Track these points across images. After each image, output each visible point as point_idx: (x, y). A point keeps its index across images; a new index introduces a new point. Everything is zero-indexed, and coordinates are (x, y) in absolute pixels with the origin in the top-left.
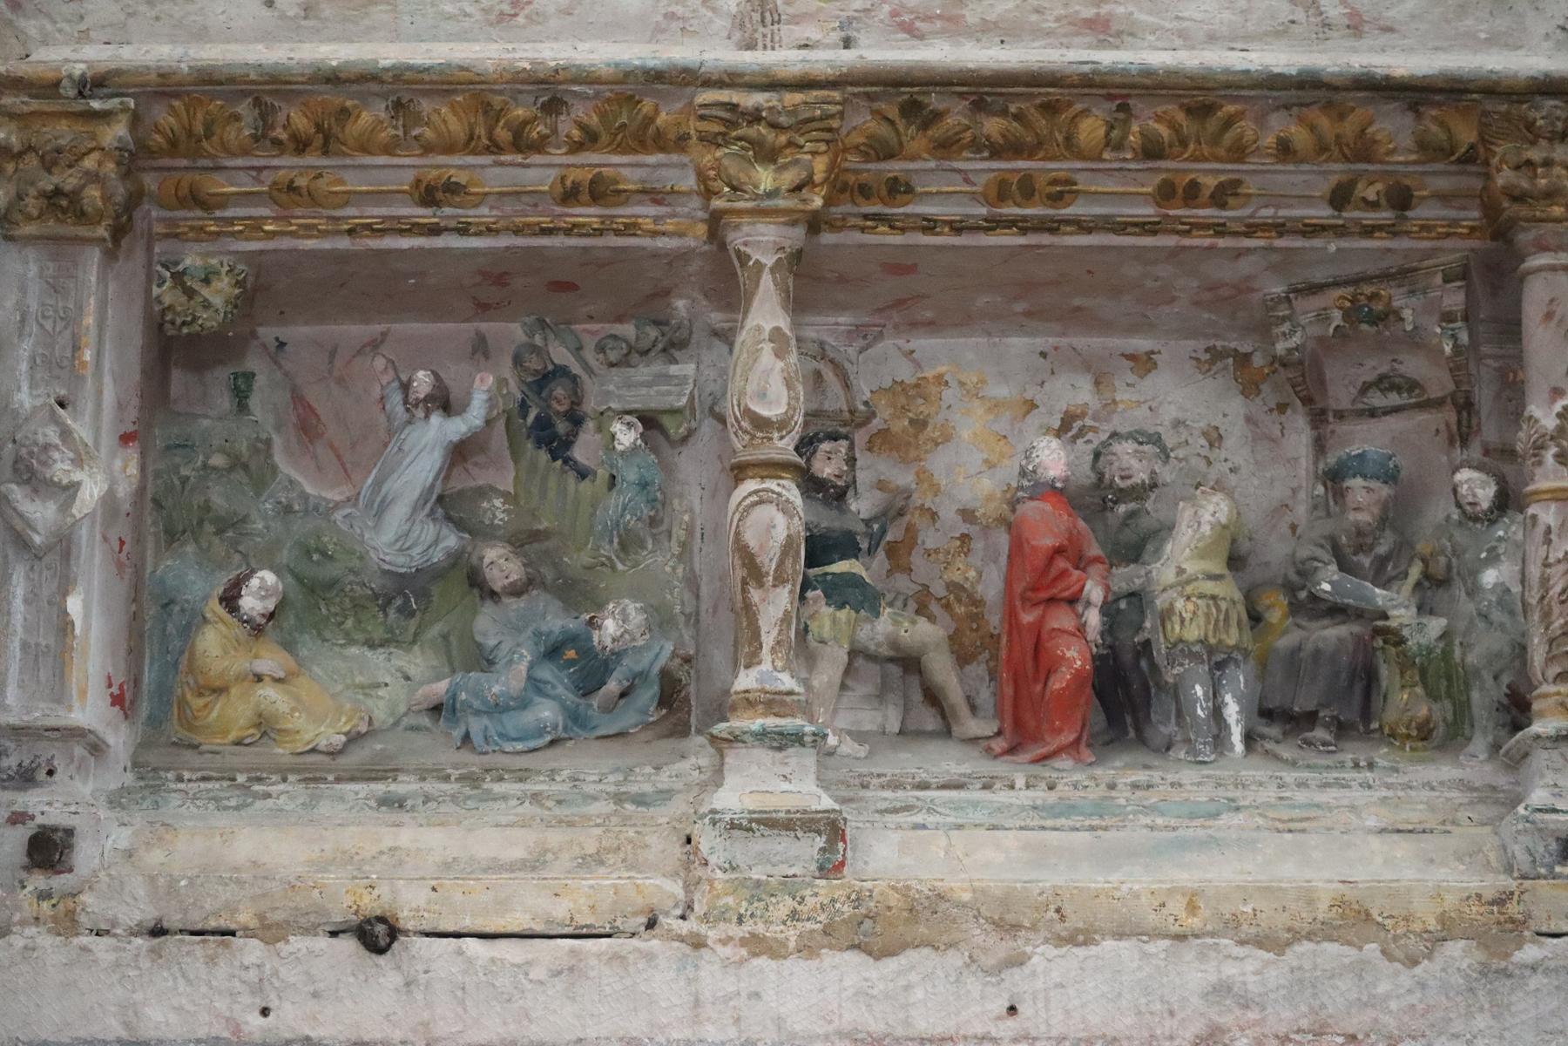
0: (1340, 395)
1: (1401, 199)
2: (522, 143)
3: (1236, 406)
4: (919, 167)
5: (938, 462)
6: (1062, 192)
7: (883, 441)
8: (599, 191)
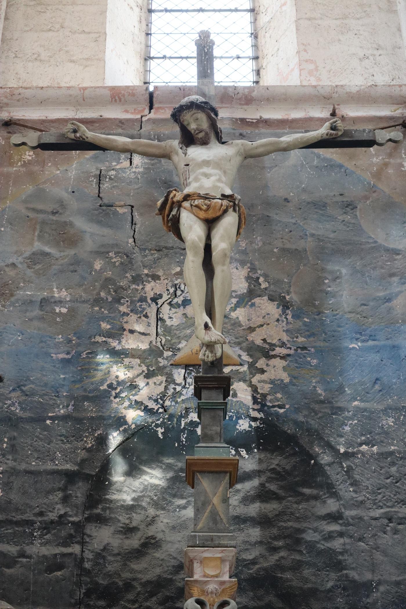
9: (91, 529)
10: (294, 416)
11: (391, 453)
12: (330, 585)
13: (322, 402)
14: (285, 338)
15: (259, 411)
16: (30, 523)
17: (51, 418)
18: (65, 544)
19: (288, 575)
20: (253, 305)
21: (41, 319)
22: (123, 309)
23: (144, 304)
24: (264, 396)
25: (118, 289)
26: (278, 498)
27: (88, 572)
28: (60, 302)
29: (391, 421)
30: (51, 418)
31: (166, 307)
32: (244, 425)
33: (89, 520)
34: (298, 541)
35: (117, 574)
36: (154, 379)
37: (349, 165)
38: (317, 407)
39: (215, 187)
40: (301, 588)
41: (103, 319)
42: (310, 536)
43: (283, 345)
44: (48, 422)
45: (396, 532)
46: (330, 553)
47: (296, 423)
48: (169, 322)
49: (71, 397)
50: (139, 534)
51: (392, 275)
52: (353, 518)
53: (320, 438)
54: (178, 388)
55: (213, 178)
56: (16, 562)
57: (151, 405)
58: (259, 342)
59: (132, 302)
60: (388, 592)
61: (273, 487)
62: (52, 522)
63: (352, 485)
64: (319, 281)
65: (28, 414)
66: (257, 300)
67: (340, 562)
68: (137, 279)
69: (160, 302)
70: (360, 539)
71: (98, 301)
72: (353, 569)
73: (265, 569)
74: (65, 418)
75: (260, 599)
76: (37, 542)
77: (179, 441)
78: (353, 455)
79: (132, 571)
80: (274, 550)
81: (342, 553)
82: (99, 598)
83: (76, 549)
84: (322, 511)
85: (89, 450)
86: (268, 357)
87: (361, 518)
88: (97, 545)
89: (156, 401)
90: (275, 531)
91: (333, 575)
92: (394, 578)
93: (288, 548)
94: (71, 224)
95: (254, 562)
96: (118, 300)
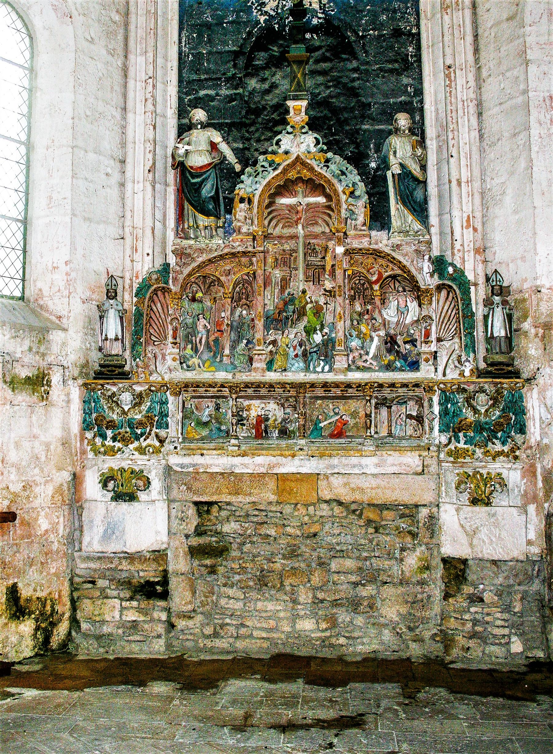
0: (286, 406)
1: (289, 391)
2: (214, 387)
5: (251, 412)
8: (221, 391)
10: (338, 16)
11: (384, 35)
12: (352, 104)
13: (352, 7)
15: (322, 13)
16: (220, 79)
17: (226, 23)
18: (236, 89)
19: (334, 100)
24: (325, 5)
26: (330, 60)
27: (246, 102)
30: (226, 23)
32: (315, 21)
33: (245, 76)
34: (339, 83)
35: (259, 102)
42: (344, 80)
44: (225, 25)
45: (383, 77)
46: (353, 88)
47: (340, 20)
49: (233, 11)
52: (364, 70)
56: (215, 99)
57: (272, 13)
60: (379, 108)
61: (328, 54)
62: (230, 77)
63: (364, 53)
65: (215, 22)
70: (368, 81)
72: (364, 97)
73: (324, 97)
75: (322, 112)
77: (285, 31)
78: (366, 36)
79: (265, 100)
80: (328, 87)
81: (358, 89)
83: (240, 91)
84: (350, 66)
85: (244, 39)
88: (250, 88)
89: (274, 10)
93: (335, 86)
95: (319, 94)
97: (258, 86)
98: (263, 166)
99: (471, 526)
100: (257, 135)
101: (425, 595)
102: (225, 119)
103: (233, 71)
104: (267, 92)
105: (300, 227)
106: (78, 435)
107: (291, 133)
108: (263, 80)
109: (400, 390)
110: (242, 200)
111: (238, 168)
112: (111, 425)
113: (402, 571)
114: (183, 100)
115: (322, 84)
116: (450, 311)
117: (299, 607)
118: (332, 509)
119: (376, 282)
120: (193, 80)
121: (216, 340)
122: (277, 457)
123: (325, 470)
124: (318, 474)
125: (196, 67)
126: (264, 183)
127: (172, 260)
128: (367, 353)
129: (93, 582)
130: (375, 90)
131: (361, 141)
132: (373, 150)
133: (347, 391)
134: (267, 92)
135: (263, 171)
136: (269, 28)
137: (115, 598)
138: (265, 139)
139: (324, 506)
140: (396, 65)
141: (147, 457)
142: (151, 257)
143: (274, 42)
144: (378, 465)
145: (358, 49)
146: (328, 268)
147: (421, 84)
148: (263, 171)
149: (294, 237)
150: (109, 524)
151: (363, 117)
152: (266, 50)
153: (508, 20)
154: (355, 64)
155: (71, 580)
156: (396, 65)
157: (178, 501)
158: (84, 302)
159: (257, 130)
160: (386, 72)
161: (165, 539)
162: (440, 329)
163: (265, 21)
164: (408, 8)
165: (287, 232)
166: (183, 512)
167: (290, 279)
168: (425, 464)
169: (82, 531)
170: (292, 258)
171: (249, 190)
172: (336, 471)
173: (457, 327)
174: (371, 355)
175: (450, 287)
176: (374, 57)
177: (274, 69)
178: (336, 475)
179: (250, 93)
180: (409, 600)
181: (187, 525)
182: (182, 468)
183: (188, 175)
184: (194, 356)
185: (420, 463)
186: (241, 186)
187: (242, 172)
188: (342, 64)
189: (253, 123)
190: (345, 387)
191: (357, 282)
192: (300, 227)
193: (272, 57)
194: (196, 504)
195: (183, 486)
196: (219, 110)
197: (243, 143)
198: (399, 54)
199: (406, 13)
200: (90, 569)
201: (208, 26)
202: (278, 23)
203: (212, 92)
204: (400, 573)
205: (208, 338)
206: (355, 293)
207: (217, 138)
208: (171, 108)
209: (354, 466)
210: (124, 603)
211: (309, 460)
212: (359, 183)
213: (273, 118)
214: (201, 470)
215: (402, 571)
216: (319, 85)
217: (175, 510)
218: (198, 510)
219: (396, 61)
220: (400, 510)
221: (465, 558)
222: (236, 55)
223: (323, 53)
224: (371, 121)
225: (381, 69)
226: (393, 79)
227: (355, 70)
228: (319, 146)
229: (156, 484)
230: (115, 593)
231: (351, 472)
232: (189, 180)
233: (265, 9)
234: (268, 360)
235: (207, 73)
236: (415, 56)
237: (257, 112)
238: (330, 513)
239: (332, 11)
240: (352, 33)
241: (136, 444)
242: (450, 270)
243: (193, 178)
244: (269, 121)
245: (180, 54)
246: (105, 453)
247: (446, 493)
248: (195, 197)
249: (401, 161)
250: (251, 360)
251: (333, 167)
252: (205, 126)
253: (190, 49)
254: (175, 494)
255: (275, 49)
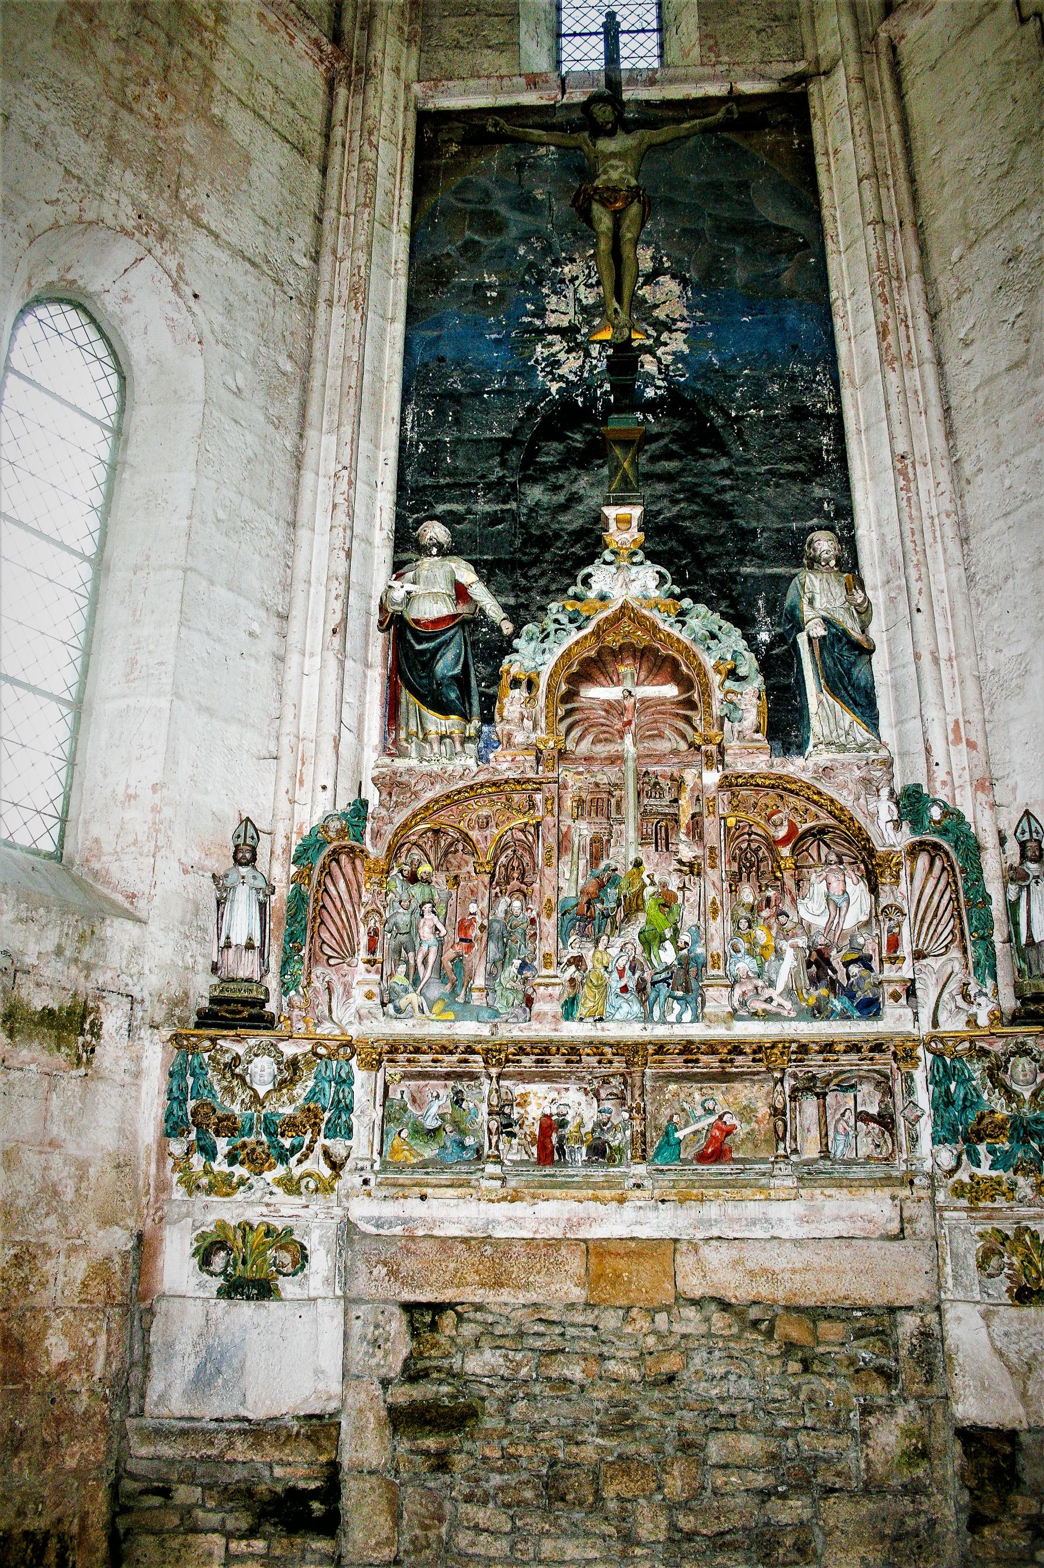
1: (610, 1062)
2: (451, 1053)
3: (584, 1098)
4: (523, 1058)
5: (528, 1109)
6: (547, 1062)
7: (518, 1105)
8: (466, 1061)
9: (526, 488)
10: (692, 384)
11: (776, 417)
12: (722, 531)
13: (717, 371)
14: (685, 313)
17: (488, 393)
18: (505, 502)
20: (657, 283)
21: (474, 302)
22: (545, 291)
23: (563, 287)
24: (667, 366)
25: (540, 272)
26: (680, 458)
27: (523, 525)
28: (490, 287)
29: (776, 388)
30: (488, 393)
31: (582, 288)
32: (650, 393)
34: (697, 494)
35: (547, 525)
36: (574, 354)
37: (744, 145)
38: (712, 375)
39: (622, 180)
40: (698, 535)
41: (528, 301)
42: (706, 490)
43: (683, 319)
45: (777, 485)
46: (722, 504)
47: (695, 390)
48: (585, 302)
49: (502, 374)
50: (564, 492)
51: (780, 252)
52: (742, 473)
53: (715, 403)
54: (594, 362)
55: (621, 170)
57: (572, 378)
58: (662, 317)
59: (553, 284)
60: (769, 538)
61: (674, 447)
64: (715, 258)
65: (468, 390)
66: (661, 279)
67: (731, 512)
68: (556, 263)
69: (577, 283)
70: (748, 492)
71: (523, 285)
72: (743, 518)
73: (669, 519)
74: (498, 392)
75: (665, 544)
76: (481, 501)
77: (596, 409)
78: (743, 418)
79: (559, 522)
80: (675, 502)
81: (732, 505)
82: (533, 546)
83: (513, 505)
85: (521, 420)
86: (671, 331)
87: (749, 474)
88: (530, 501)
90: (677, 485)
91: (725, 523)
92: (776, 526)
93: (686, 499)
94: (497, 213)
95: (659, 512)
96: (540, 283)
97: (545, 499)
98: (556, 621)
99: (1019, 1352)
100: (542, 582)
101: (923, 1519)
102: (481, 553)
103: (498, 472)
104: (564, 508)
105: (628, 739)
106: (155, 1147)
107: (611, 563)
108: (556, 488)
109: (844, 1058)
110: (515, 683)
111: (507, 628)
112: (228, 1126)
113: (868, 1462)
114: (406, 520)
115: (664, 496)
116: (936, 898)
117: (638, 1551)
118: (707, 1320)
119: (785, 841)
120: (425, 487)
121: (458, 961)
122: (586, 1203)
123: (691, 1231)
124: (676, 1241)
125: (430, 463)
126: (559, 651)
127: (372, 795)
128: (772, 984)
129: (165, 1492)
130: (762, 506)
131: (739, 595)
132: (762, 611)
133: (732, 1061)
134: (564, 508)
135: (556, 631)
136: (566, 402)
137: (214, 1531)
138: (558, 590)
139: (690, 1312)
140: (801, 467)
141: (303, 1200)
142: (330, 791)
143: (575, 426)
144: (804, 1220)
145: (729, 438)
146: (685, 819)
147: (849, 497)
148: (556, 631)
149: (616, 759)
150: (209, 1349)
151: (743, 552)
152: (562, 438)
153: (1009, 369)
154: (724, 463)
155: (115, 1488)
156: (801, 467)
157: (367, 1302)
158: (186, 872)
159: (543, 574)
160: (782, 476)
161: (336, 1388)
162: (919, 934)
163: (558, 391)
164: (817, 373)
165: (602, 750)
166: (377, 1326)
167: (609, 841)
168: (906, 1214)
169: (147, 1368)
170: (613, 801)
171: (529, 664)
172: (715, 1232)
173: (954, 927)
174: (780, 986)
175: (936, 846)
176: (759, 452)
177: (574, 471)
178: (713, 1243)
179: (531, 510)
180: (887, 1531)
181: (385, 1356)
182: (378, 1226)
183: (410, 637)
184: (411, 989)
185: (895, 1214)
186: (514, 657)
187: (517, 634)
188: (700, 463)
189: (536, 561)
190: (730, 1053)
191: (744, 846)
192: (628, 739)
193: (570, 451)
194: (408, 1307)
195: (380, 1267)
196: (471, 537)
197: (517, 596)
198: (805, 448)
199: (814, 381)
200: (159, 1458)
201: (454, 397)
202: (582, 394)
203: (459, 508)
204: (863, 1466)
205: (440, 953)
206: (740, 868)
207: (467, 575)
208: (381, 529)
209: (754, 1222)
210: (233, 1545)
211: (656, 1208)
212: (745, 653)
213: (573, 553)
214: (420, 1232)
215: (868, 1462)
216: (659, 498)
217: (359, 1322)
218: (411, 1322)
219: (799, 459)
220: (857, 1319)
221: (1010, 1427)
222: (505, 445)
223: (666, 445)
224: (756, 560)
225: (770, 472)
226: (796, 489)
227: (725, 473)
228: (666, 587)
229: (320, 1262)
230: (215, 1519)
231: (747, 1235)
232: (413, 647)
233: (560, 372)
234: (565, 997)
235: (451, 474)
236: (834, 451)
237: (544, 542)
238: (703, 1329)
239: (681, 376)
240: (717, 412)
241: (280, 1170)
242: (936, 813)
243: (420, 643)
244: (566, 558)
245: (402, 440)
246: (210, 1189)
247: (955, 1278)
248: (421, 678)
249: (824, 614)
250: (529, 1001)
251: (693, 622)
252: (444, 552)
253: (421, 435)
254: (361, 1285)
255: (578, 437)
